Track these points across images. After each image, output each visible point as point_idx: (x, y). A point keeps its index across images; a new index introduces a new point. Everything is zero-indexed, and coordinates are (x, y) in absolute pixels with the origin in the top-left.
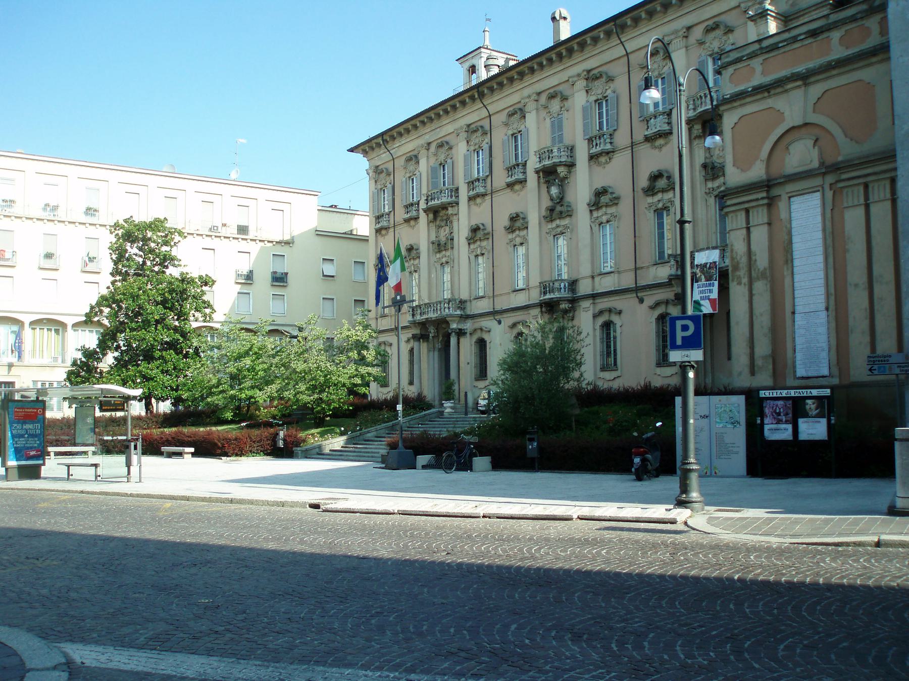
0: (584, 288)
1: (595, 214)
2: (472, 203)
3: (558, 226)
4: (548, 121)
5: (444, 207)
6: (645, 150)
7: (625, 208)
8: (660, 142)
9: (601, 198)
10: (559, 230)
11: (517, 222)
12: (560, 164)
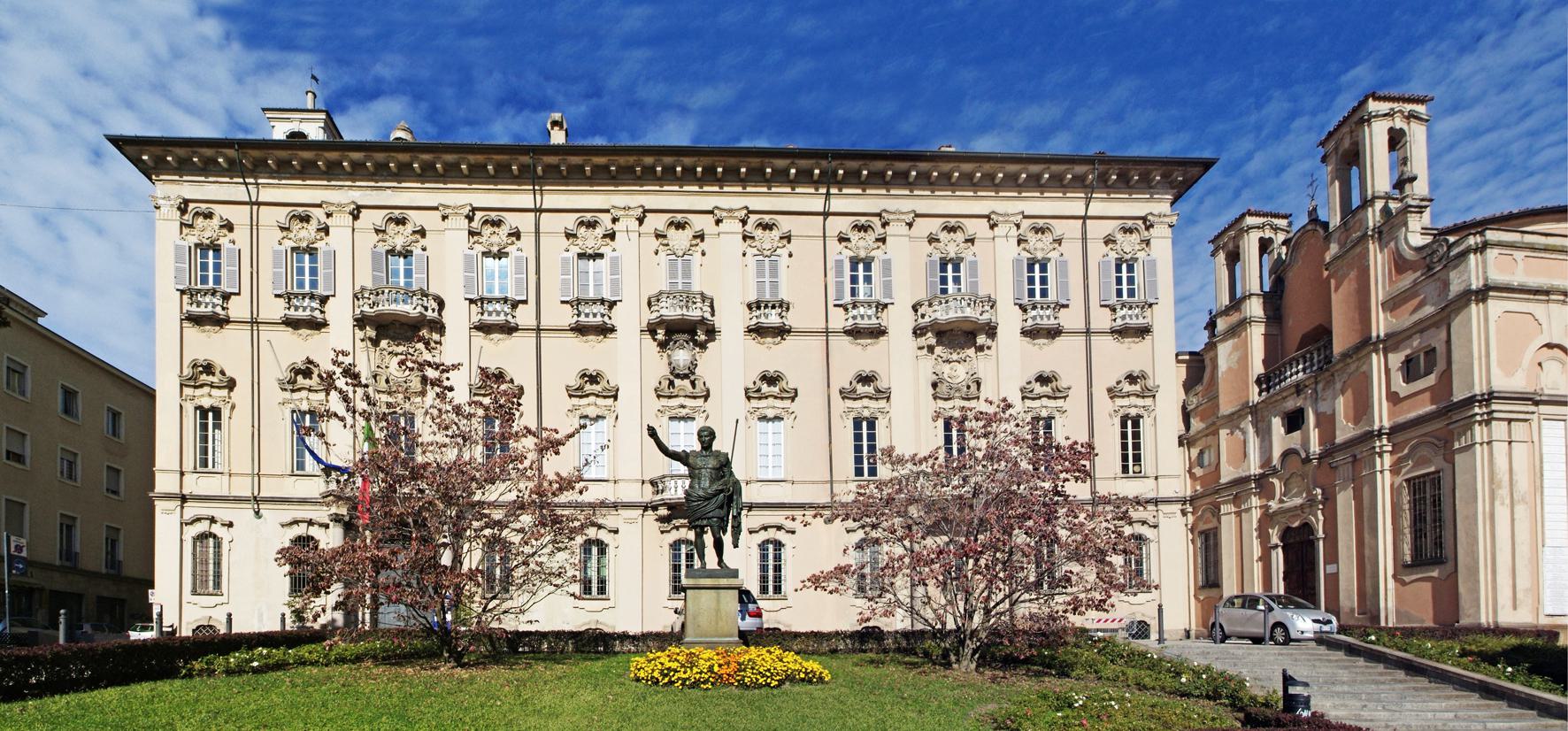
2: (474, 333)
3: (683, 407)
6: (841, 344)
7: (810, 404)
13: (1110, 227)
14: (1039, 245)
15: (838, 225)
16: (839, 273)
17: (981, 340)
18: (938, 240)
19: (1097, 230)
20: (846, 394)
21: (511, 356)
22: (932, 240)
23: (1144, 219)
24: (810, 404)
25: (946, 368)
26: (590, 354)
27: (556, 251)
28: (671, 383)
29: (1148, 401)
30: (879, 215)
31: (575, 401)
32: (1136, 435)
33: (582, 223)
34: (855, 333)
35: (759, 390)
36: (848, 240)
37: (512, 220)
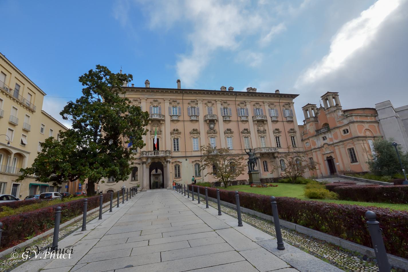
1: (226, 135)
3: (212, 135)
5: (159, 121)
6: (240, 123)
7: (236, 134)
10: (213, 136)
11: (195, 132)
12: (216, 120)
15: (238, 103)
16: (239, 111)
17: (265, 122)
19: (282, 104)
20: (242, 133)
21: (179, 126)
22: (254, 105)
24: (236, 134)
25: (259, 128)
26: (195, 126)
27: (186, 106)
29: (295, 134)
30: (245, 101)
31: (192, 135)
32: (294, 140)
36: (240, 105)
37: (178, 101)
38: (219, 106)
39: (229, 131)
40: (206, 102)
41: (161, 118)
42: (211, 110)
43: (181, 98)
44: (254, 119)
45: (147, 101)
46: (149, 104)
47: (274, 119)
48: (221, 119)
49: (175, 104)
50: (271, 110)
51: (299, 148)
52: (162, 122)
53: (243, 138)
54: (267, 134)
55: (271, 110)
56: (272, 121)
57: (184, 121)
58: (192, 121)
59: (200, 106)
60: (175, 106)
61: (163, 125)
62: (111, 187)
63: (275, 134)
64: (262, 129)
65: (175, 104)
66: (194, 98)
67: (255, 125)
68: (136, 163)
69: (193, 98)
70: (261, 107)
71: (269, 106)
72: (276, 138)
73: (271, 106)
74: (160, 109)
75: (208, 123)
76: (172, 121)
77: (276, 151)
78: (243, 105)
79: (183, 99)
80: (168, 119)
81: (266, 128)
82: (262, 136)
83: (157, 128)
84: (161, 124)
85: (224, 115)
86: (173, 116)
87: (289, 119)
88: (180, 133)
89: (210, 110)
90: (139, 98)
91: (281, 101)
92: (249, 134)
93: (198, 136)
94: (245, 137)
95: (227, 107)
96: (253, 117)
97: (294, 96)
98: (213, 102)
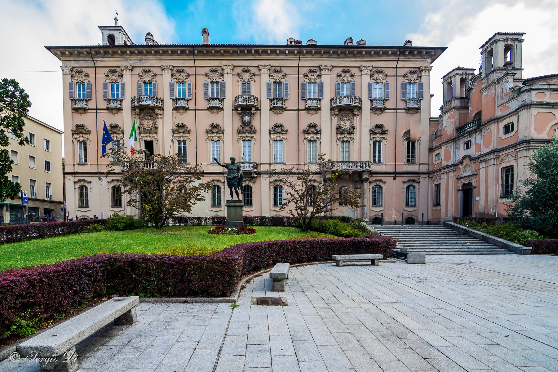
0: (265, 168)
1: (272, 135)
3: (247, 137)
4: (240, 83)
6: (303, 114)
7: (292, 136)
8: (314, 112)
9: (278, 130)
10: (247, 138)
11: (215, 130)
12: (253, 106)
13: (405, 71)
14: (379, 78)
15: (304, 71)
17: (355, 112)
18: (340, 76)
19: (401, 72)
20: (305, 132)
21: (187, 119)
22: (338, 76)
23: (419, 68)
24: (292, 136)
25: (342, 123)
26: (215, 118)
28: (243, 128)
30: (319, 67)
31: (209, 135)
32: (413, 148)
33: (212, 71)
34: (308, 109)
35: (274, 131)
36: (307, 76)
37: (187, 70)
38: (264, 78)
39: (280, 130)
40: (239, 70)
41: (155, 103)
42: (249, 88)
43: (192, 63)
44: (333, 105)
45: (134, 73)
46: (137, 79)
47: (376, 104)
48: (265, 105)
49: (181, 77)
50: (374, 86)
51: (419, 165)
52: (157, 111)
53: (306, 142)
54: (356, 136)
55: (374, 86)
56: (371, 109)
57: (196, 109)
58: (210, 109)
59: (228, 79)
60: (181, 81)
61: (159, 116)
62: (84, 214)
63: (372, 136)
64: (346, 125)
65: (181, 77)
66: (216, 63)
67: (334, 116)
68: (118, 181)
69: (214, 62)
70: (354, 79)
71: (371, 77)
72: (375, 144)
73: (376, 76)
74: (155, 87)
75: (239, 114)
76: (176, 109)
77: (364, 169)
78: (315, 75)
79: (195, 67)
80: (168, 105)
81: (356, 123)
82: (345, 139)
83: (151, 122)
84: (157, 115)
85: (272, 97)
86: (176, 99)
87: (411, 104)
88: (189, 132)
89: (247, 87)
90: (119, 67)
91: (400, 64)
92: (318, 136)
93: (221, 137)
94: (310, 141)
95: (282, 81)
96: (331, 101)
97: (434, 53)
98: (253, 70)
